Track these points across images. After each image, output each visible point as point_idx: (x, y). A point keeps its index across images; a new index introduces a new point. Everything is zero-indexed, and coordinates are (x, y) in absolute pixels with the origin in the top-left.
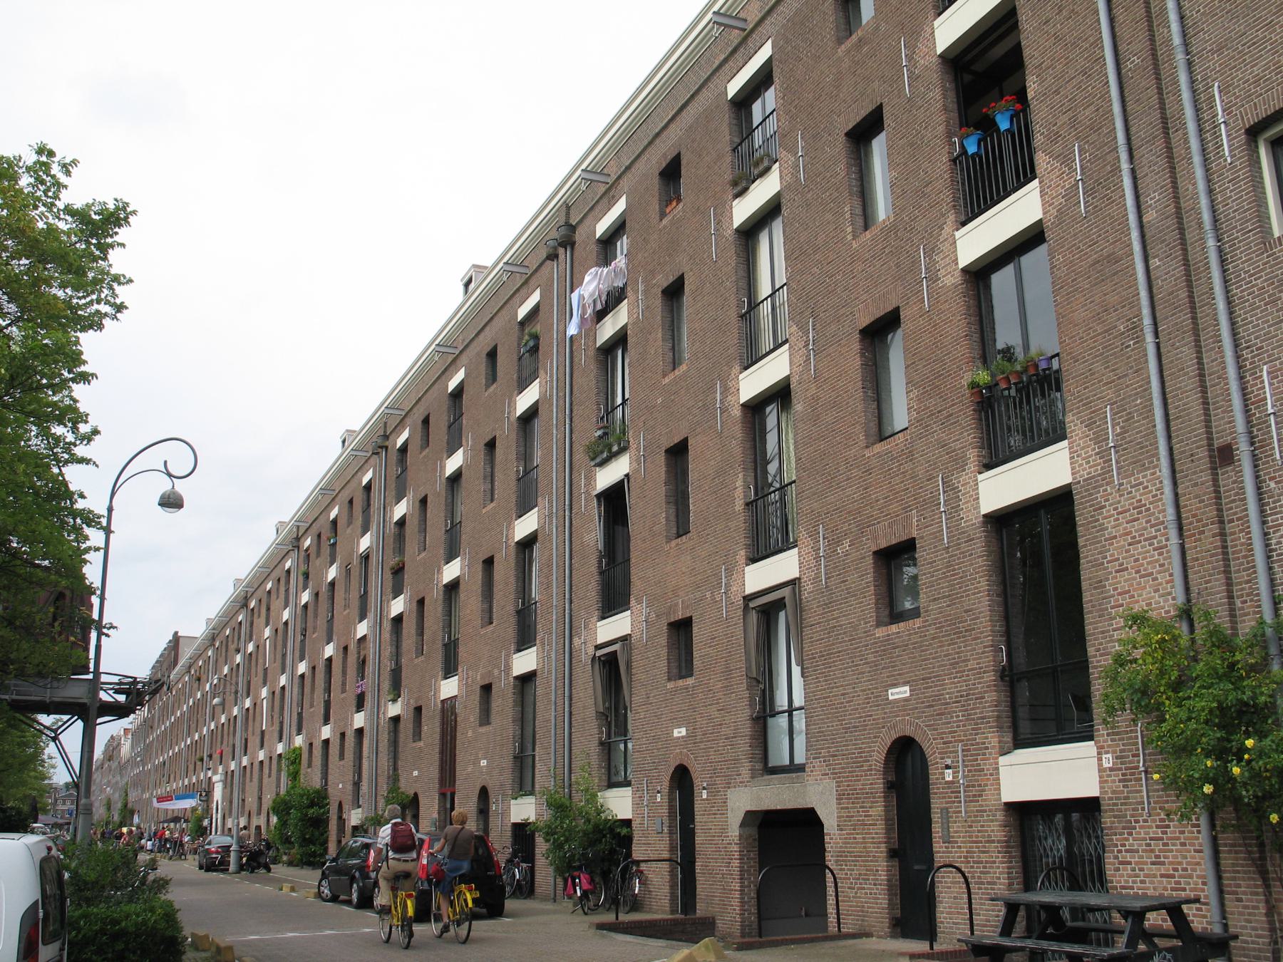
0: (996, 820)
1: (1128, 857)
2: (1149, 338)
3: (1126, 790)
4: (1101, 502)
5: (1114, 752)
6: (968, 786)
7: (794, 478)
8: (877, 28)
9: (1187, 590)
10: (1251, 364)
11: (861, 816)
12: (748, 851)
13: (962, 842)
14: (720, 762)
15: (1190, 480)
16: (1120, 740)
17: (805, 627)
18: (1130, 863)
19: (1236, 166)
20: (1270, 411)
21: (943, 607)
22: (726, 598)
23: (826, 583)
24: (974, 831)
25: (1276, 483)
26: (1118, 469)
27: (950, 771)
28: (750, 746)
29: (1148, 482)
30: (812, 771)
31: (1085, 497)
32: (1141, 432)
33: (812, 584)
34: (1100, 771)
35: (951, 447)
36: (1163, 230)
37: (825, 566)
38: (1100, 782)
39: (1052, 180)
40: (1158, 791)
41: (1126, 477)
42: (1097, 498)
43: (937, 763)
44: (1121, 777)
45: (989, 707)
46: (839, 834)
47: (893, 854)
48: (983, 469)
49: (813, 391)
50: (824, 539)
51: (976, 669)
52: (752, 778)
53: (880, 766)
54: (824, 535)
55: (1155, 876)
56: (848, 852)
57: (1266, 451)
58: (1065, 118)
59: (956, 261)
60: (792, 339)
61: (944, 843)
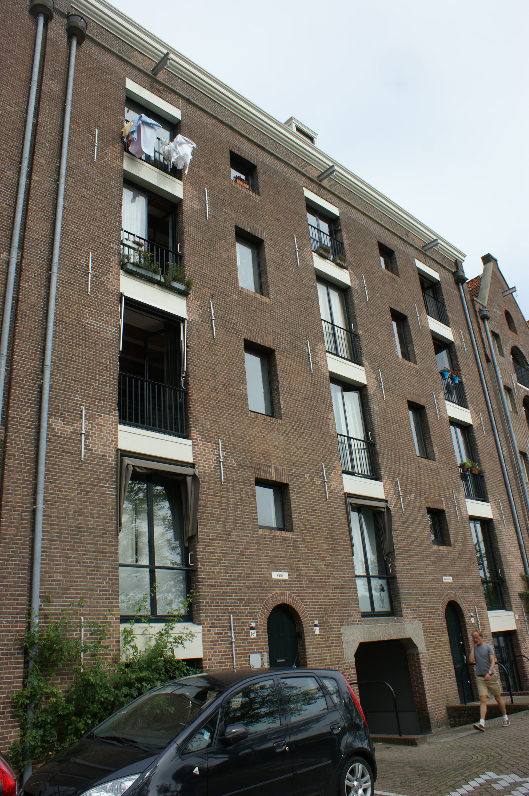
14: (331, 605)
30: (406, 616)
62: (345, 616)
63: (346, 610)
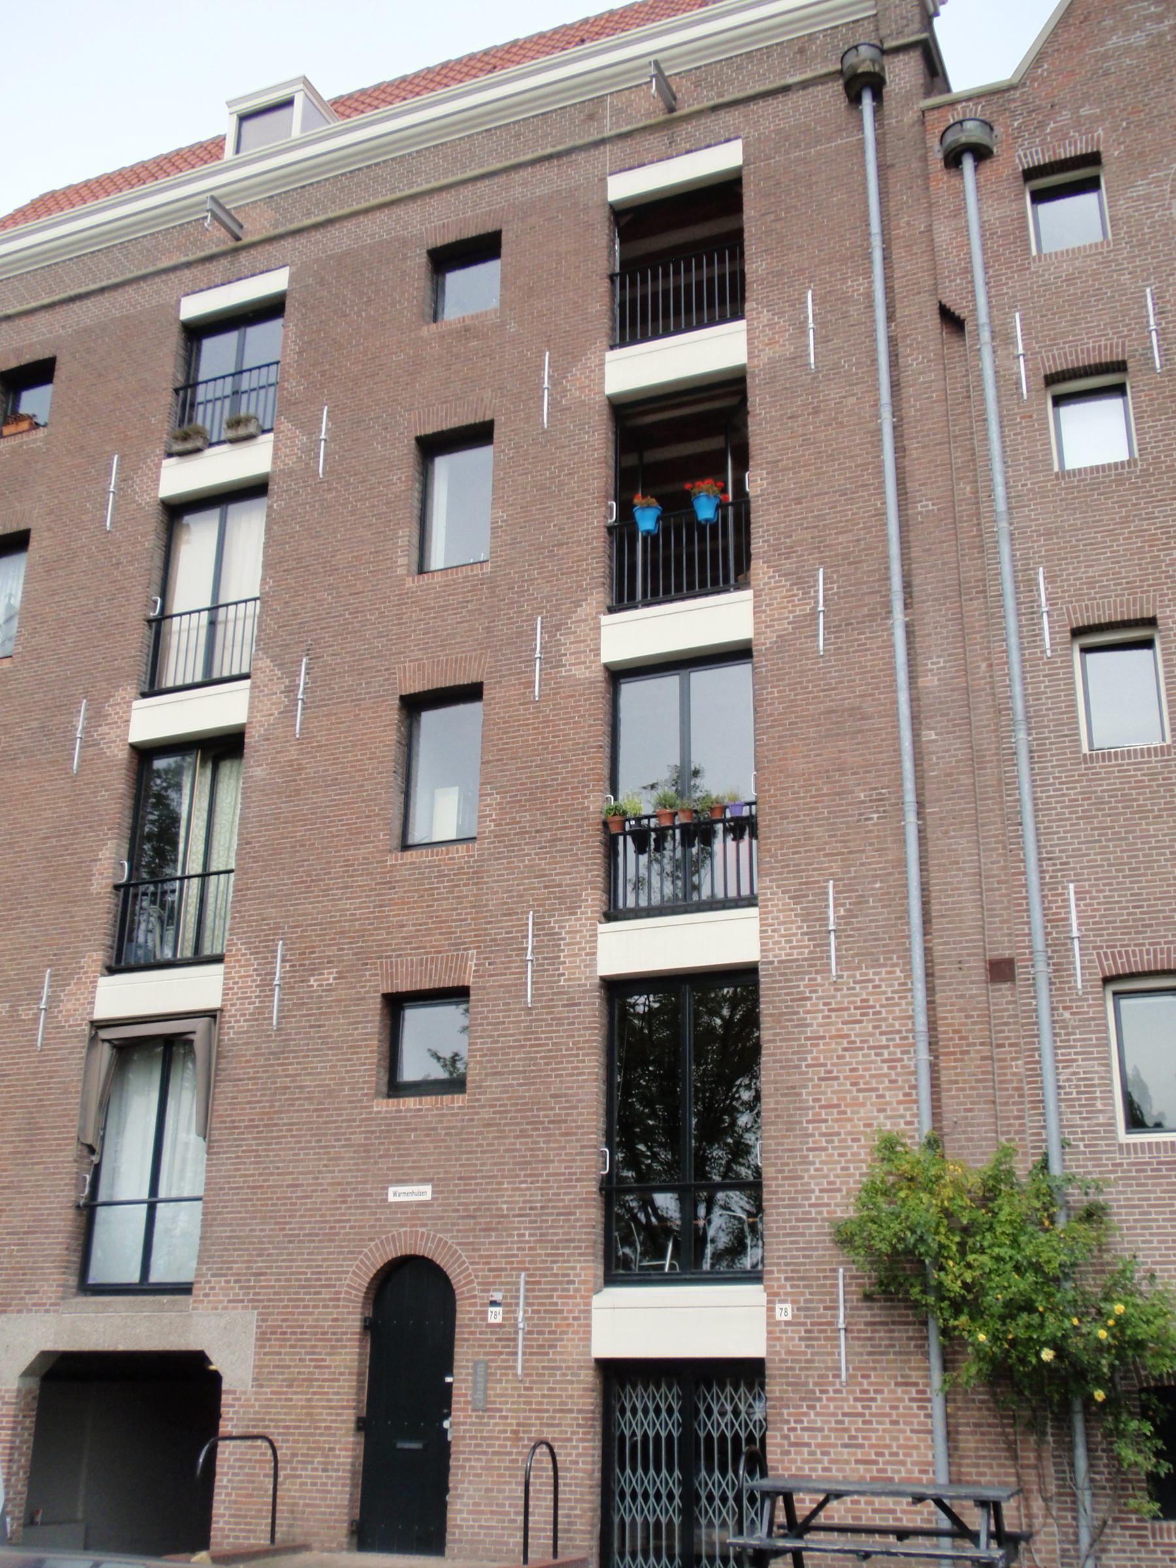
0: (579, 1382)
1: (806, 1437)
2: (911, 818)
3: (809, 1351)
4: (804, 992)
5: (793, 1302)
6: (530, 1332)
7: (233, 866)
8: (503, 324)
9: (936, 1116)
10: (1051, 877)
11: (308, 1367)
12: (24, 1416)
13: (510, 1410)
15: (955, 990)
16: (805, 1286)
17: (220, 1081)
18: (808, 1445)
19: (1056, 662)
20: (831, 927)
21: (511, 1085)
22: (46, 1018)
23: (278, 1023)
24: (536, 1396)
25: (1072, 1014)
26: (837, 957)
27: (499, 1310)
28: (67, 1249)
29: (881, 980)
30: (206, 1295)
31: (780, 981)
32: (877, 921)
33: (245, 1021)
34: (768, 1324)
35: (554, 880)
36: (947, 702)
37: (281, 1000)
38: (769, 1339)
39: (776, 598)
40: (861, 1354)
41: (848, 969)
42: (798, 986)
43: (475, 1297)
44: (803, 1334)
45: (582, 1227)
46: (256, 1393)
47: (362, 1425)
48: (603, 919)
49: (293, 754)
50: (283, 961)
51: (564, 1174)
52: (63, 1298)
53: (358, 1295)
54: (283, 956)
55: (847, 1462)
56: (271, 1420)
57: (1063, 976)
58: (807, 535)
59: (597, 651)
60: (258, 676)
61: (473, 1410)
62: (19, 1293)
63: (22, 1281)
